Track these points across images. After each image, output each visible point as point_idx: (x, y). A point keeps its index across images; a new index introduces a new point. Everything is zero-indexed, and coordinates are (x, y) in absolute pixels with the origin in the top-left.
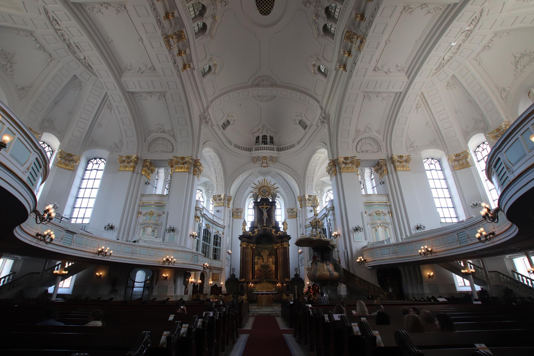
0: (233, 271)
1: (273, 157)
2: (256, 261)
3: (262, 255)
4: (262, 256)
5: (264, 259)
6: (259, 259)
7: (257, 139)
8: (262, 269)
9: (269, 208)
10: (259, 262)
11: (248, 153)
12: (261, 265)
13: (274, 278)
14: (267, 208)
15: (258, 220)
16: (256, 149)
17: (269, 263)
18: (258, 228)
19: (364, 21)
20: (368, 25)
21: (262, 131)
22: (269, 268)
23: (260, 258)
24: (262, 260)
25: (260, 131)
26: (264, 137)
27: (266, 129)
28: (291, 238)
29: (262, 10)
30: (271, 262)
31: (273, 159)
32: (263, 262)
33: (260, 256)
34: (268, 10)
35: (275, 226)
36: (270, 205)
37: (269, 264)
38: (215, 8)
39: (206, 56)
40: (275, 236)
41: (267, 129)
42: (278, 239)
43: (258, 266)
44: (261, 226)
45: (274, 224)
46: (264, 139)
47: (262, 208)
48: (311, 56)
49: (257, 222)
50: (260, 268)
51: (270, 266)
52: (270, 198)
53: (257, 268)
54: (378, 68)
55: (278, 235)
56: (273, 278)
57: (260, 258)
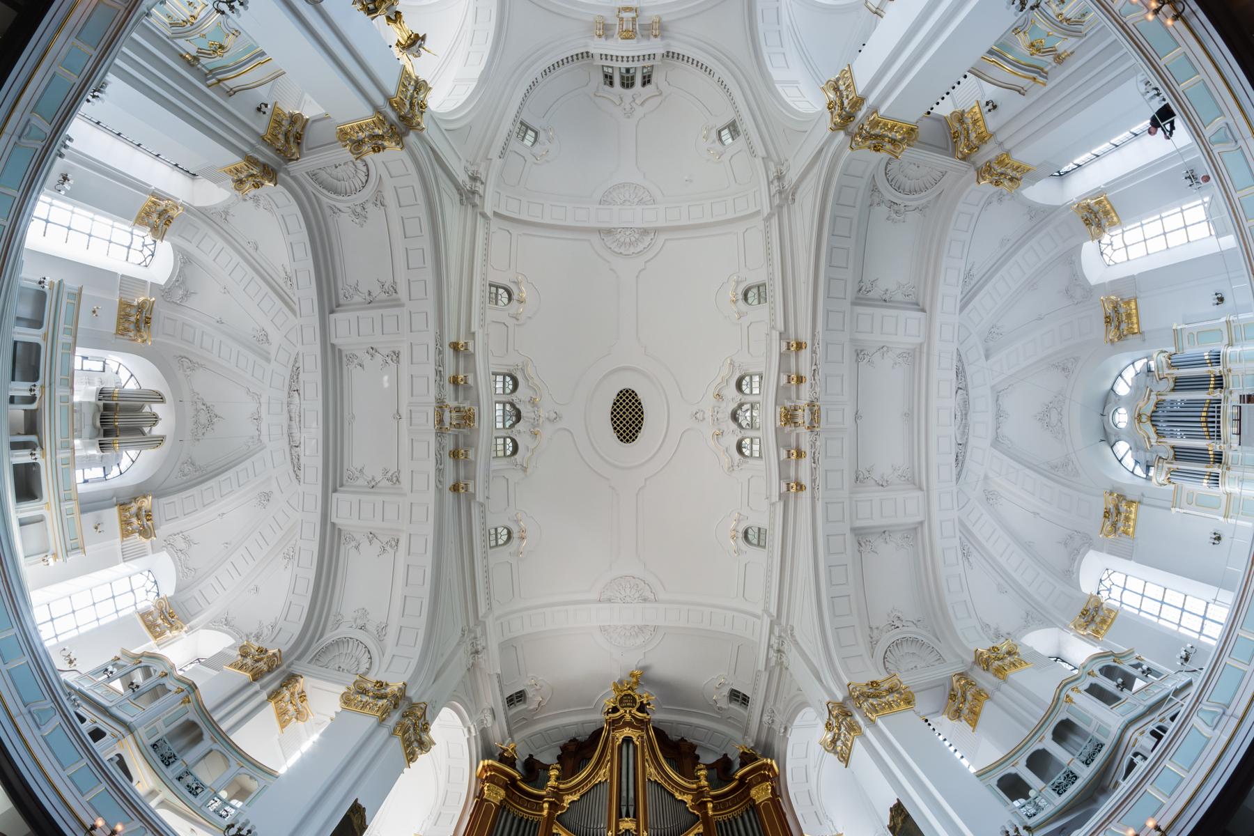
1: (603, 39)
7: (647, 79)
11: (676, 49)
16: (652, 56)
19: (450, 452)
20: (442, 452)
21: (634, 100)
25: (638, 101)
26: (628, 82)
27: (623, 104)
29: (633, 398)
31: (601, 33)
34: (621, 398)
38: (716, 413)
39: (748, 327)
41: (620, 105)
46: (628, 77)
48: (530, 318)
54: (392, 360)
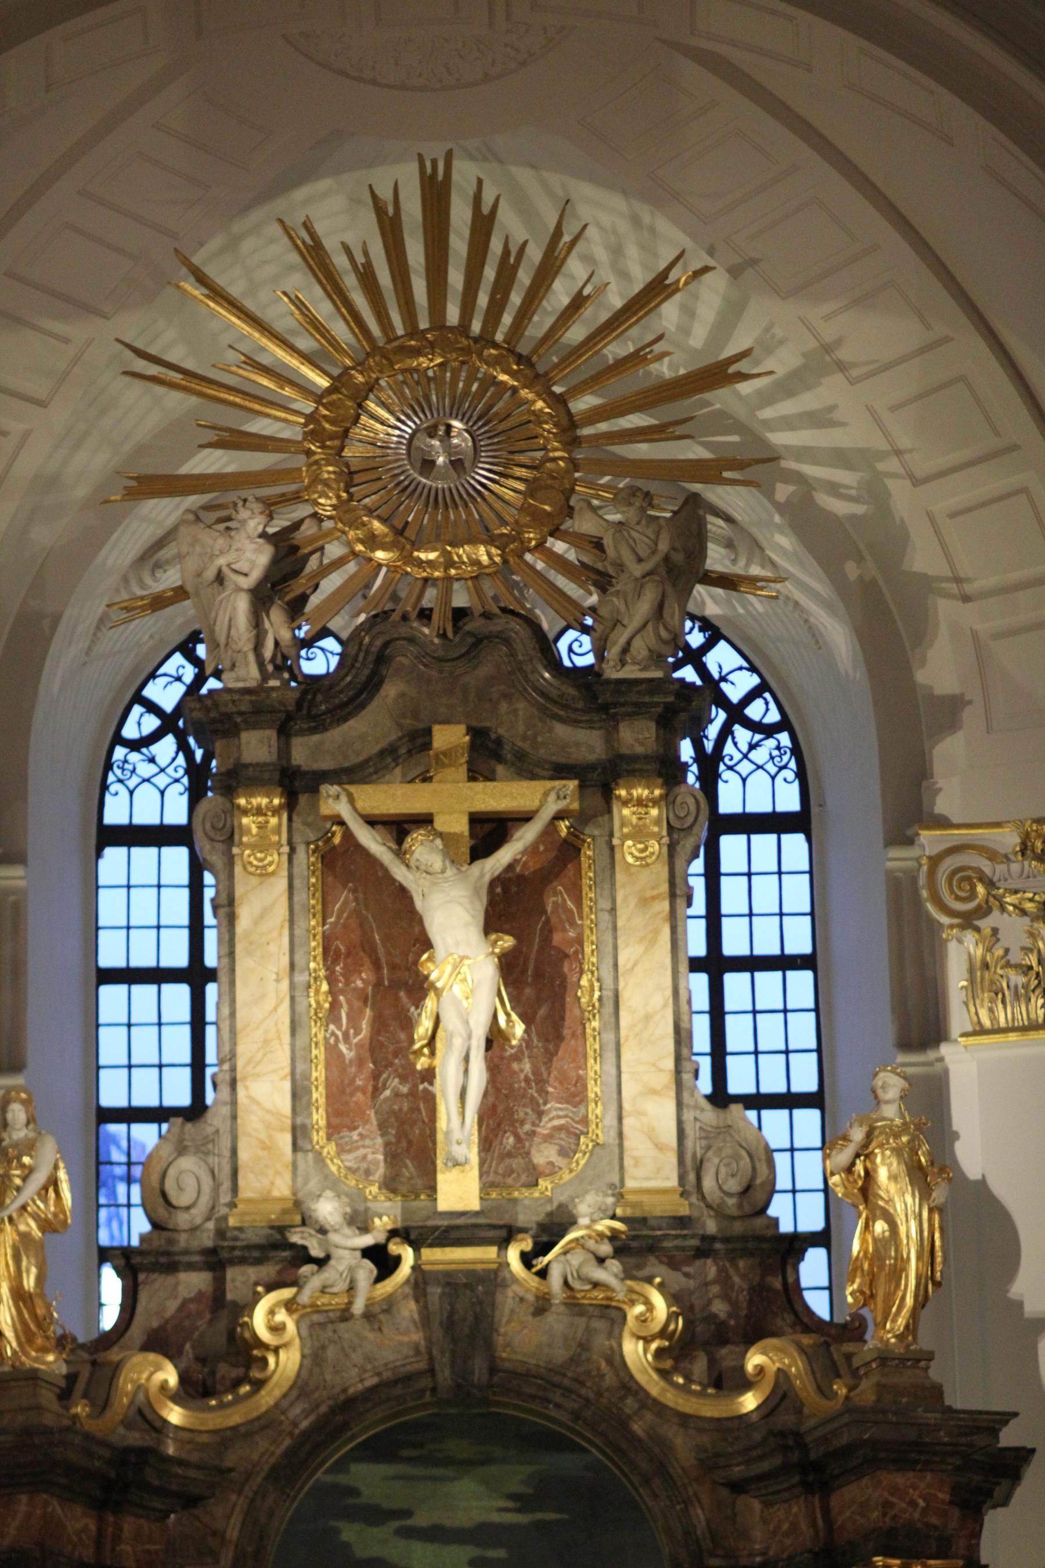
15: (318, 1095)
18: (314, 1280)
28: (1023, 1455)
35: (684, 1211)
36: (561, 771)
40: (685, 1419)
42: (738, 1487)
44: (382, 1224)
45: (673, 1182)
49: (299, 1134)
55: (749, 1402)
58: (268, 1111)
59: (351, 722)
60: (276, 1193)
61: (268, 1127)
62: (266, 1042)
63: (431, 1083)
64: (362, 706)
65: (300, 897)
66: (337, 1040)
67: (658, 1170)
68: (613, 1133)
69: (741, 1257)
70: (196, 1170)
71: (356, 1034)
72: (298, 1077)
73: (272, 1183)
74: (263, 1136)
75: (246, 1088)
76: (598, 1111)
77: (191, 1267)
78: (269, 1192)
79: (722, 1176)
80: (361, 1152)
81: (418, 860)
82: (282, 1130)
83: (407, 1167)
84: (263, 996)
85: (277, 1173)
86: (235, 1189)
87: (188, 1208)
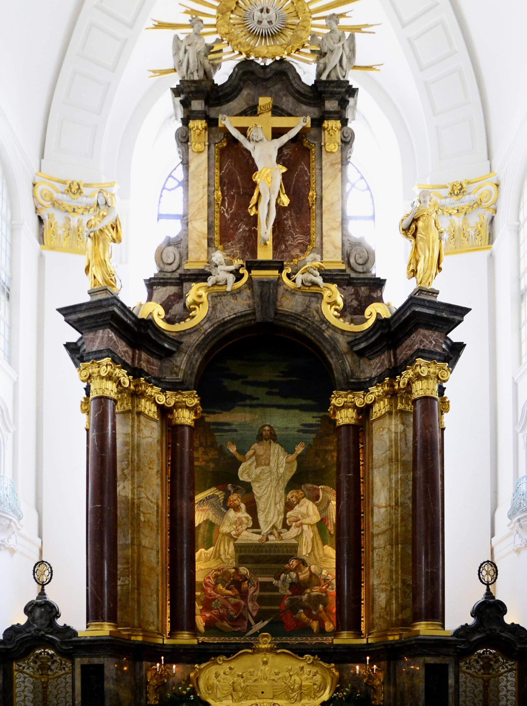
0: (44, 579)
2: (207, 521)
3: (243, 477)
4: (247, 488)
5: (261, 505)
6: (226, 506)
8: (244, 570)
9: (292, 134)
10: (225, 529)
12: (238, 548)
13: (329, 627)
14: (277, 133)
17: (294, 532)
22: (294, 563)
23: (234, 497)
24: (243, 514)
30: (309, 525)
32: (256, 525)
33: (229, 487)
37: (298, 537)
43: (217, 556)
47: (243, 131)
50: (233, 563)
51: (304, 551)
52: (308, 62)
53: (214, 564)
56: (322, 631)
57: (234, 497)
58: (199, 232)
59: (231, 103)
60: (201, 260)
61: (199, 237)
62: (199, 209)
63: (256, 227)
64: (235, 97)
65: (212, 162)
66: (224, 212)
67: (335, 255)
68: (319, 244)
69: (363, 286)
70: (174, 251)
71: (231, 210)
72: (210, 222)
73: (200, 256)
74: (197, 240)
75: (192, 224)
76: (314, 237)
77: (171, 284)
78: (199, 259)
79: (357, 258)
80: (232, 249)
81: (253, 135)
82: (204, 238)
83: (247, 255)
84: (198, 193)
85: (202, 253)
86: (187, 258)
87: (171, 264)
